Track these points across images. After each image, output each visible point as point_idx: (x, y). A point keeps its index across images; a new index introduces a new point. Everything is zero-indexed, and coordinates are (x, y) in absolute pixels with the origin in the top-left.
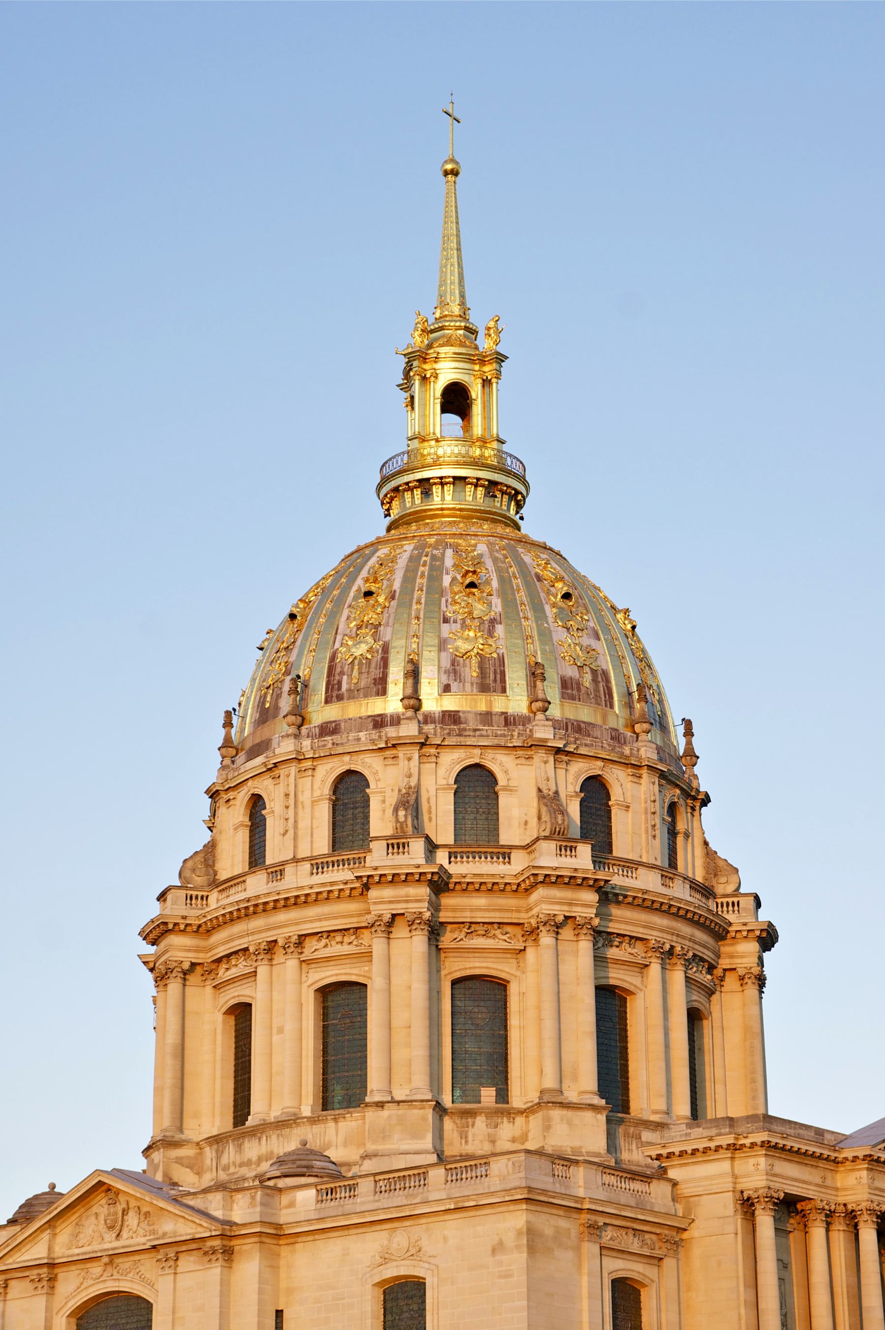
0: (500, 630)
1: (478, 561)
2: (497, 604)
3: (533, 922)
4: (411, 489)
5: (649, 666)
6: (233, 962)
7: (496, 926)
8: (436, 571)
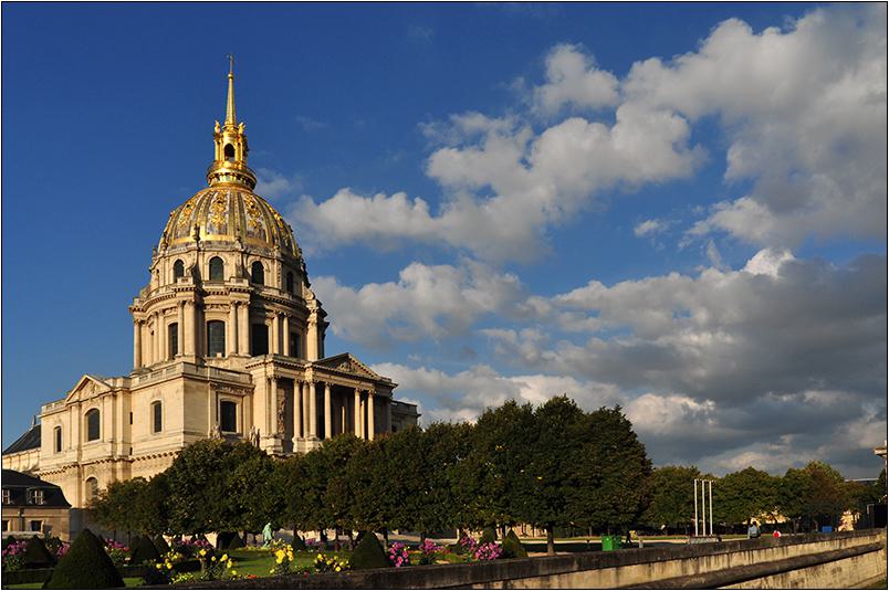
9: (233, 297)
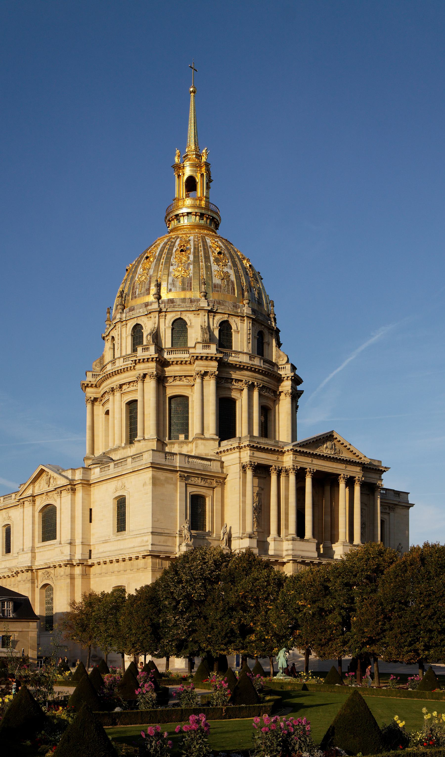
3: (195, 374)
4: (173, 220)
7: (183, 377)
9: (200, 366)
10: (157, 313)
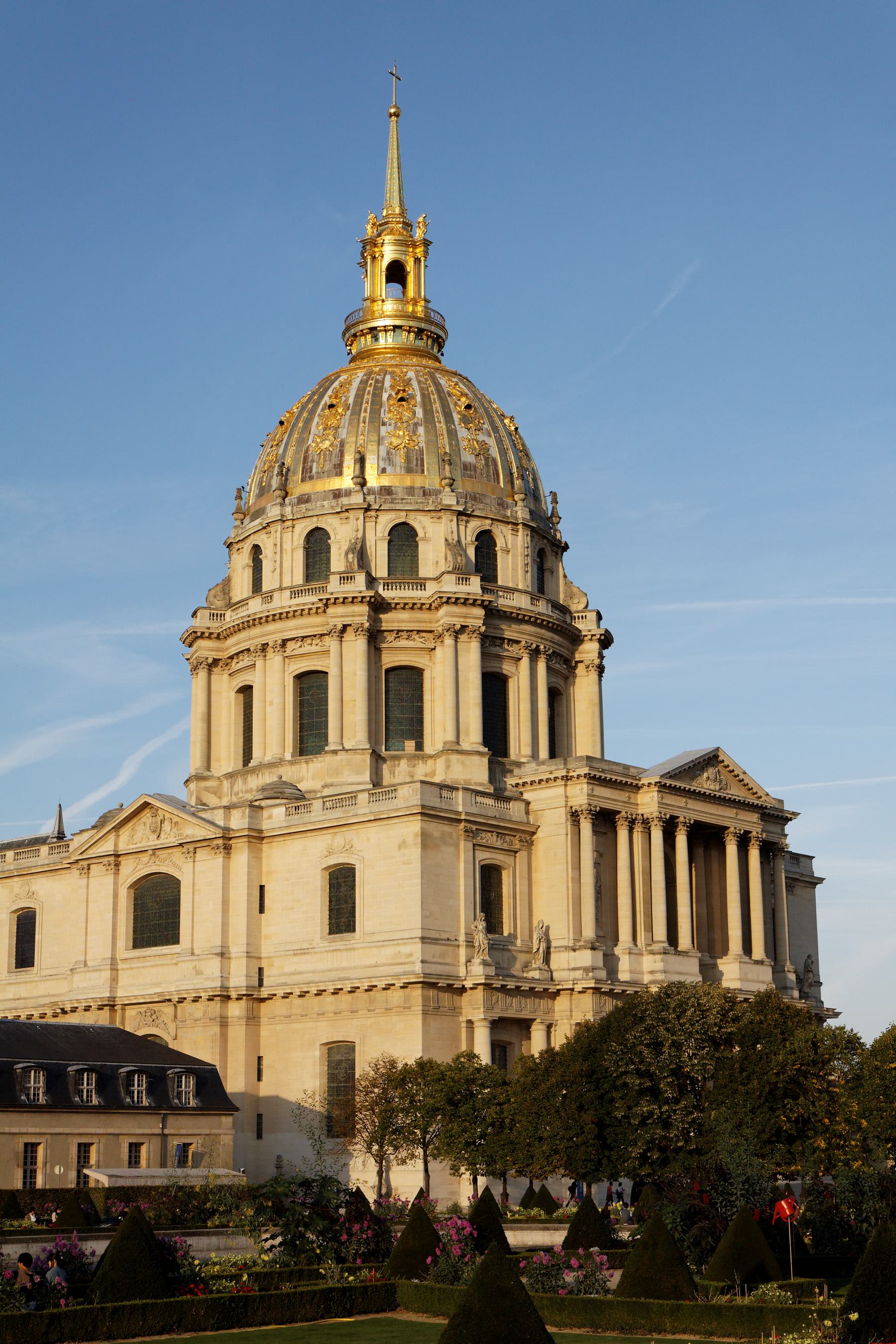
0: (421, 430)
1: (408, 382)
2: (419, 412)
3: (440, 629)
4: (363, 335)
5: (527, 456)
6: (241, 658)
7: (415, 632)
8: (379, 389)
9: (446, 616)
10: (363, 511)
